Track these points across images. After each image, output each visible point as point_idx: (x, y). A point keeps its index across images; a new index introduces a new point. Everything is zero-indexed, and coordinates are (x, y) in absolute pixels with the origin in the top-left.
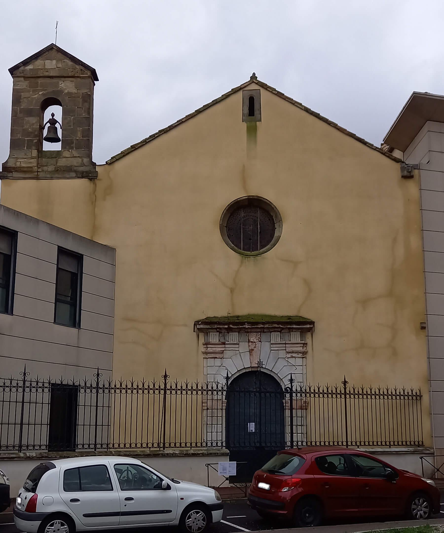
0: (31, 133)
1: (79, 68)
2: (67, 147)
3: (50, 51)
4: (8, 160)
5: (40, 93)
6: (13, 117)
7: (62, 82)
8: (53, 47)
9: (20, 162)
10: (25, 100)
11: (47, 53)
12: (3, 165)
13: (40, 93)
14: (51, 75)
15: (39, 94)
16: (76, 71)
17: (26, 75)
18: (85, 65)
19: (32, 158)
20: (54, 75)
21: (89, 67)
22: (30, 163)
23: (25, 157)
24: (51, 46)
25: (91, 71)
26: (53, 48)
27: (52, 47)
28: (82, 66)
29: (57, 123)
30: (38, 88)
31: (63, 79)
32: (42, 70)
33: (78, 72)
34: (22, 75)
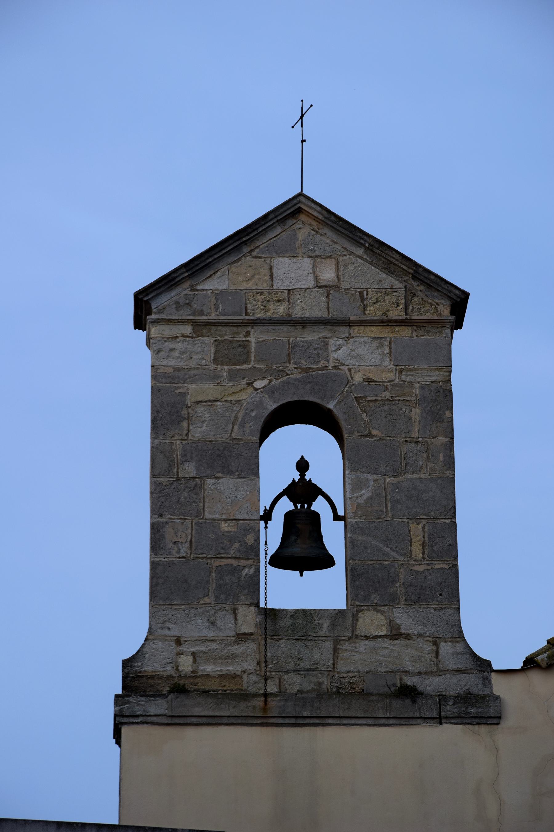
0: (232, 539)
1: (405, 287)
2: (375, 598)
3: (290, 222)
4: (143, 646)
5: (259, 384)
6: (160, 475)
7: (341, 341)
8: (300, 208)
9: (194, 654)
10: (200, 409)
11: (279, 230)
12: (126, 664)
13: (259, 384)
14: (298, 313)
15: (256, 389)
16: (394, 300)
17: (202, 313)
18: (430, 279)
19: (242, 637)
20: (310, 314)
21: (446, 286)
22: (233, 657)
23: (209, 634)
24: (296, 204)
25: (450, 298)
26: (299, 211)
27: (299, 205)
28: (414, 278)
29: (320, 498)
30: (247, 361)
31: (344, 331)
32: (262, 294)
33: (398, 306)
34: (185, 314)
